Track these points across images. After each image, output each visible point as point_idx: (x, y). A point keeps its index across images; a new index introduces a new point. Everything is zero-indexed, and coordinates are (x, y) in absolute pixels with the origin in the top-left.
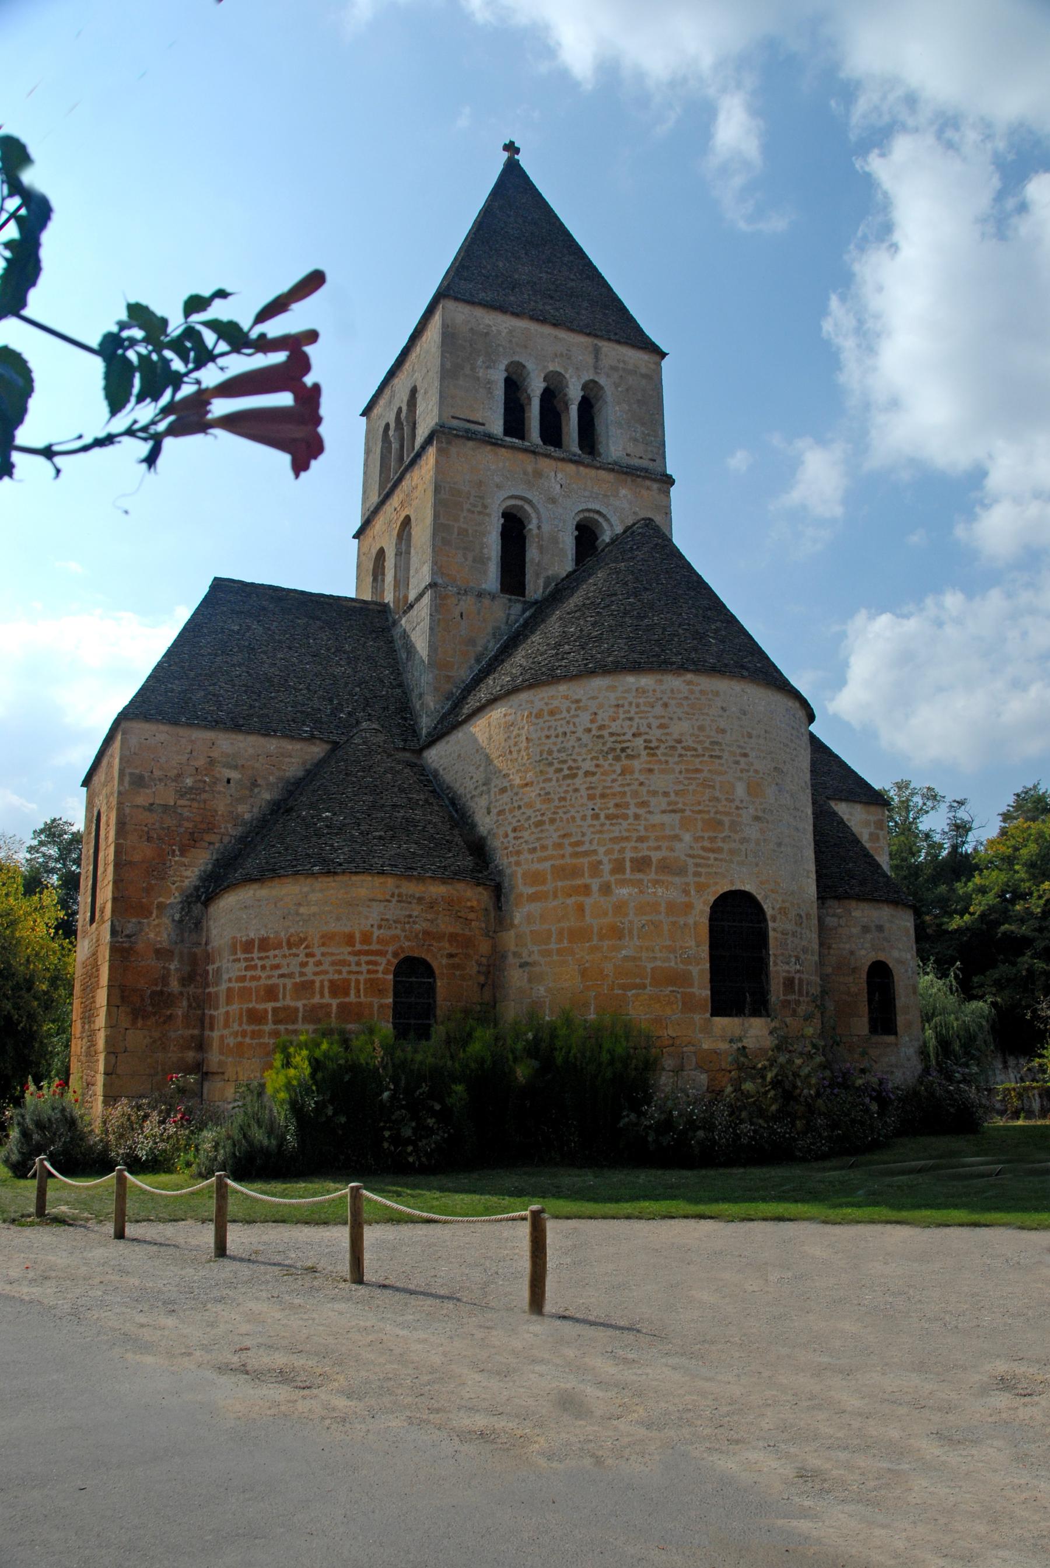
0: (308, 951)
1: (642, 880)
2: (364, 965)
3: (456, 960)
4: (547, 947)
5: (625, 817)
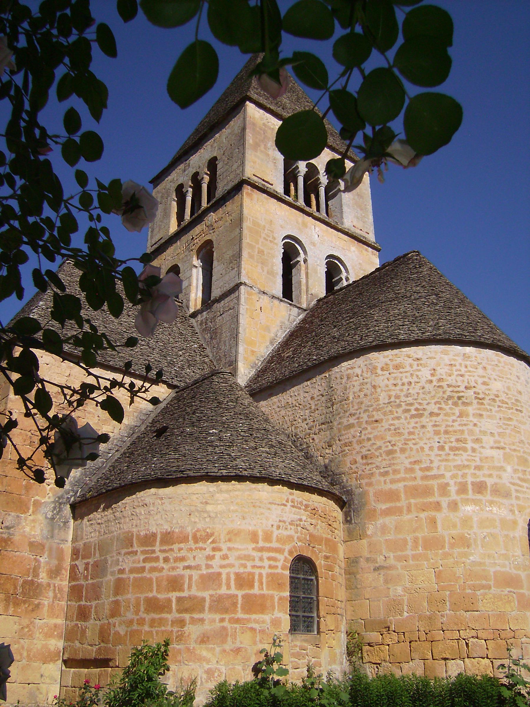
0: (214, 545)
2: (266, 560)
4: (404, 553)
5: (465, 450)
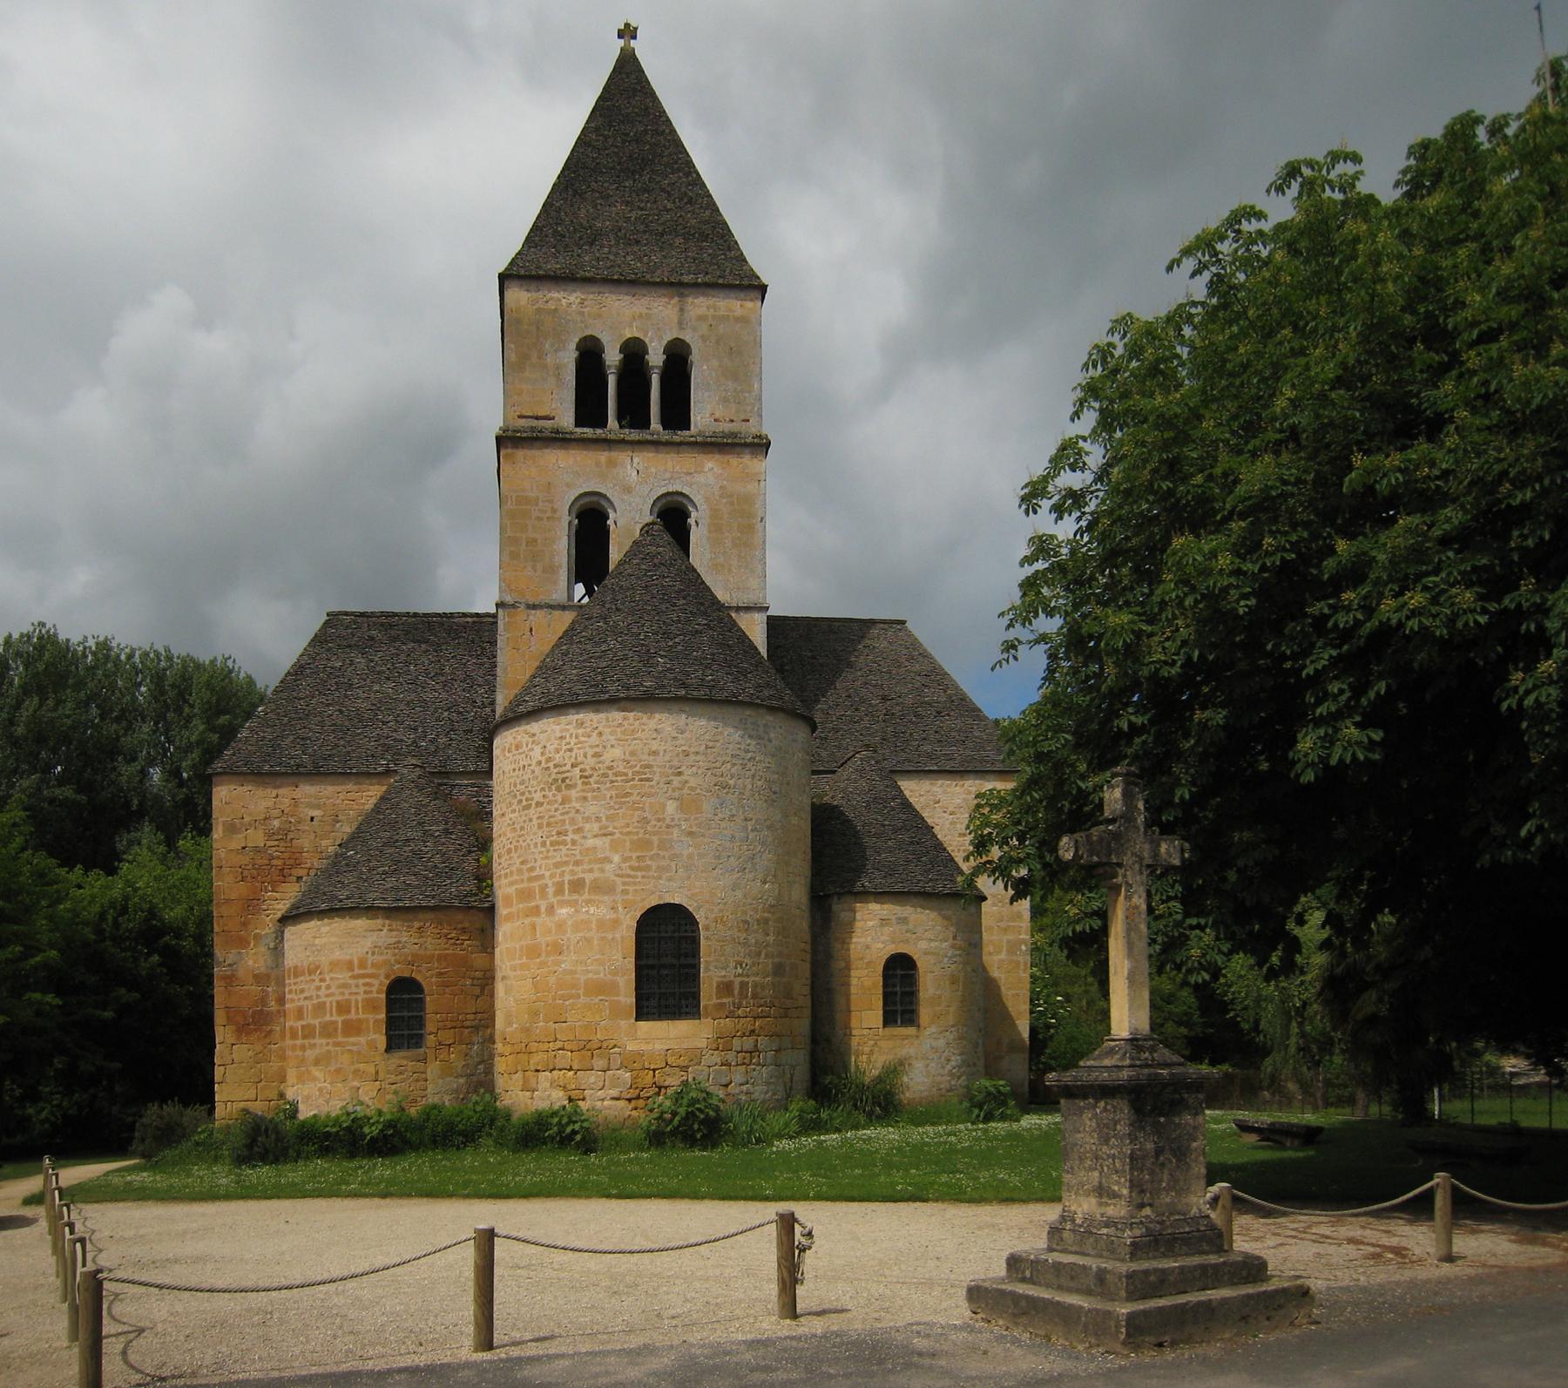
1: (576, 902)
5: (564, 843)
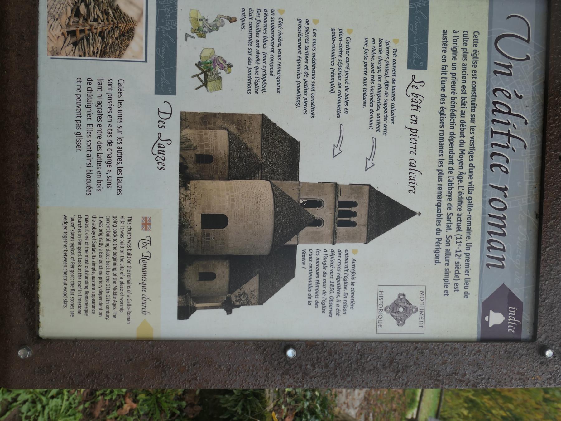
3: (213, 169)
5: (243, 197)
